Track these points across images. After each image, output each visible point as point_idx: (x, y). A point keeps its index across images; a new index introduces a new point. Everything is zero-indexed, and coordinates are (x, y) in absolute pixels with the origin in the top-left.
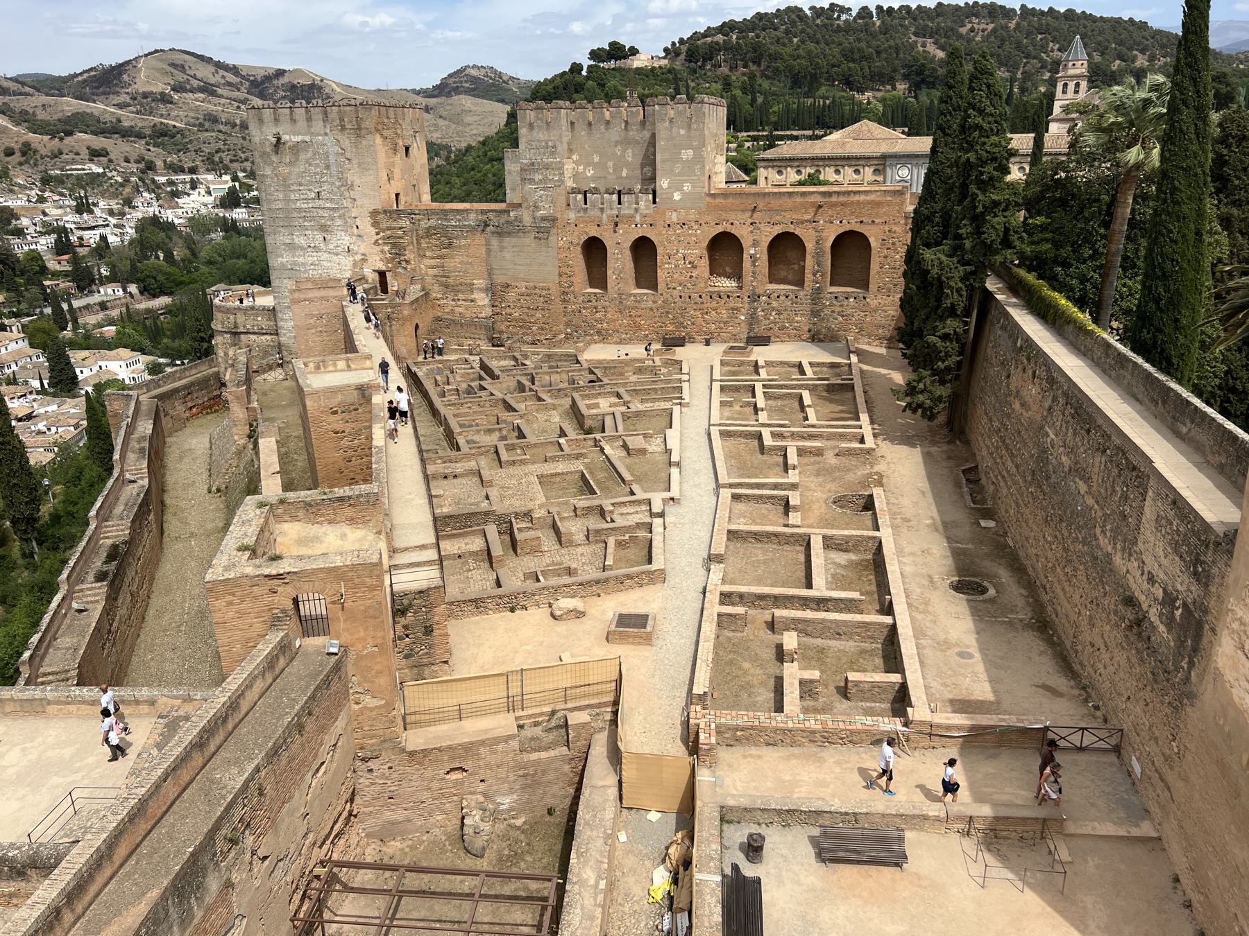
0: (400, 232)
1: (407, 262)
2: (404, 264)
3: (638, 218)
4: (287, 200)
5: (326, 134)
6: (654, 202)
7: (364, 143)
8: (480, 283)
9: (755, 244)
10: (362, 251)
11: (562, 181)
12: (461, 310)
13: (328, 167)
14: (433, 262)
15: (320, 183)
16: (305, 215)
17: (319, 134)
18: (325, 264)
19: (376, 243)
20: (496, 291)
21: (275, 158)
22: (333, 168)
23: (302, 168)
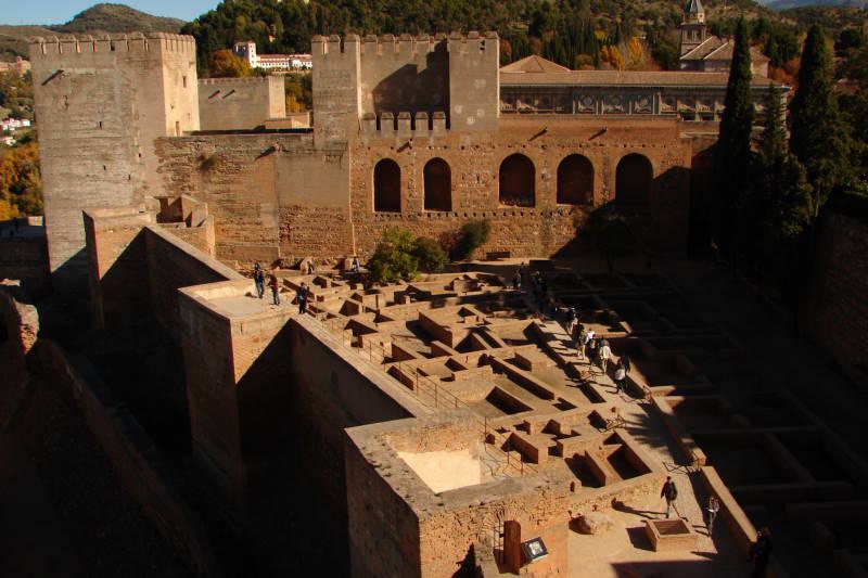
0: (185, 160)
1: (189, 187)
2: (187, 190)
3: (432, 142)
5: (112, 67)
6: (448, 126)
7: (151, 73)
8: (267, 206)
9: (547, 164)
10: (143, 178)
11: (356, 107)
12: (245, 233)
13: (112, 98)
14: (218, 187)
15: (103, 114)
16: (85, 144)
17: (105, 67)
18: (104, 192)
19: (159, 170)
20: (287, 215)
22: (117, 99)
23: (84, 99)
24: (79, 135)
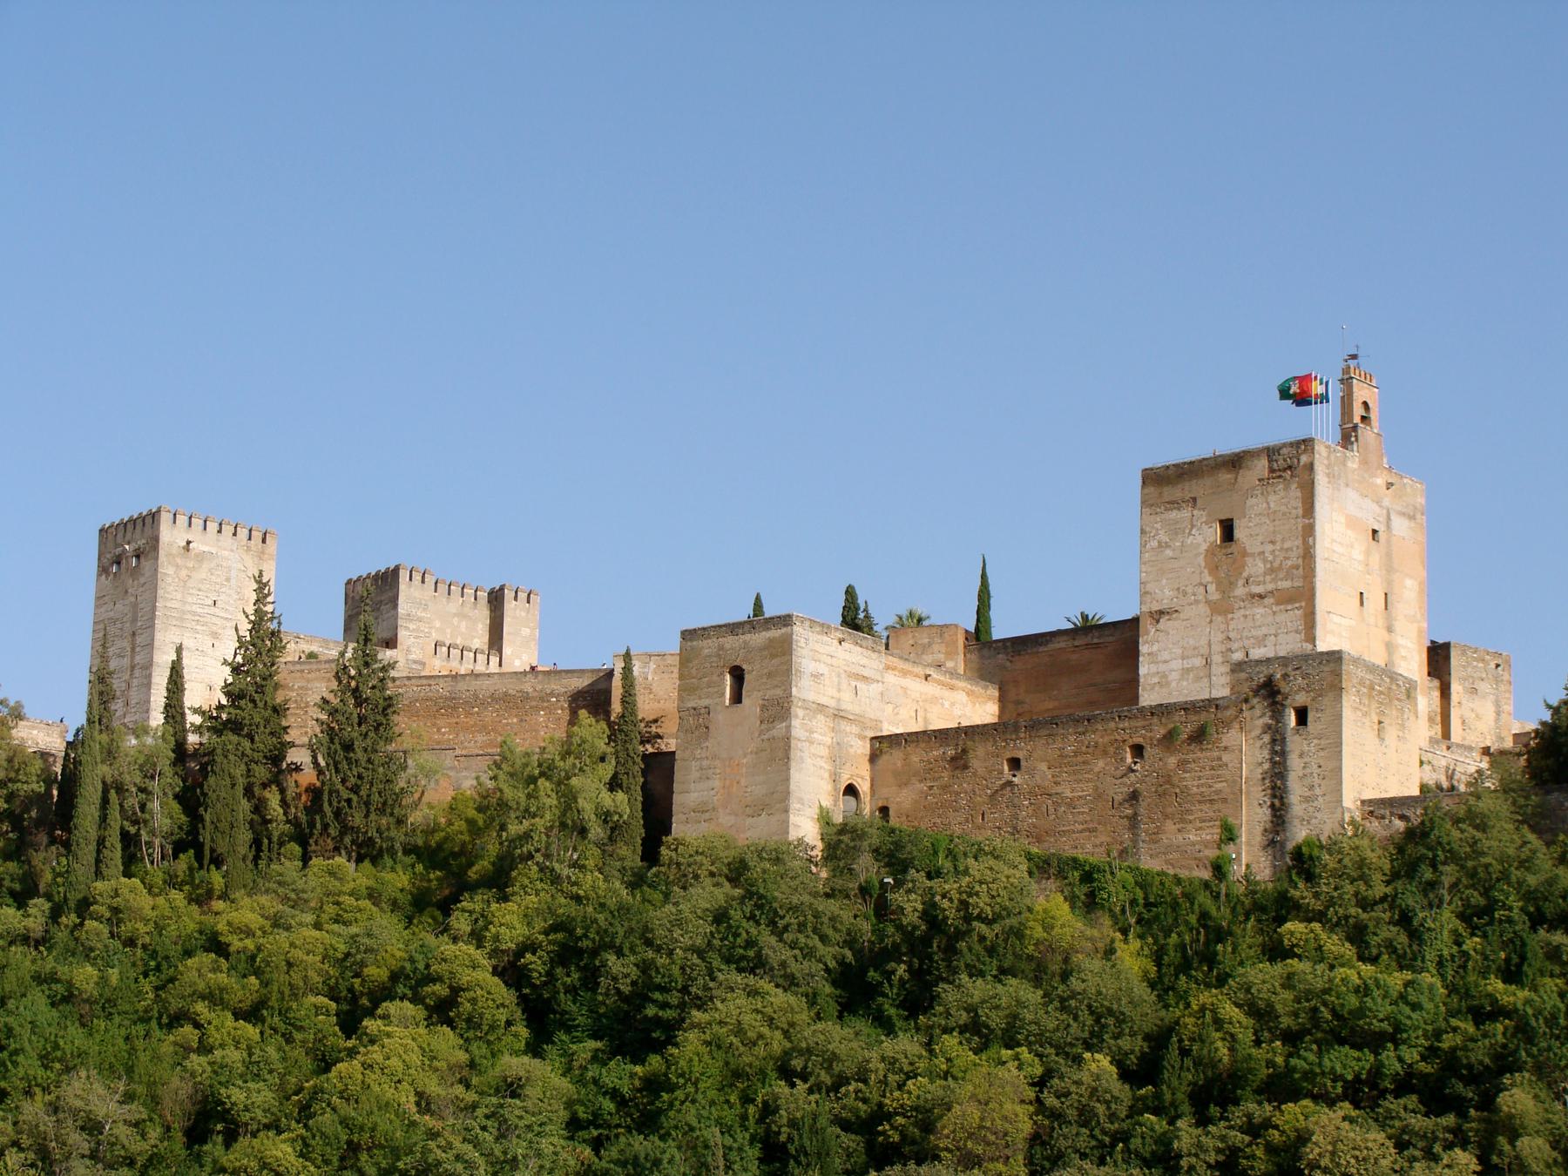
4: (184, 603)
13: (228, 580)
21: (179, 561)
22: (233, 582)
23: (203, 576)
24: (195, 608)
